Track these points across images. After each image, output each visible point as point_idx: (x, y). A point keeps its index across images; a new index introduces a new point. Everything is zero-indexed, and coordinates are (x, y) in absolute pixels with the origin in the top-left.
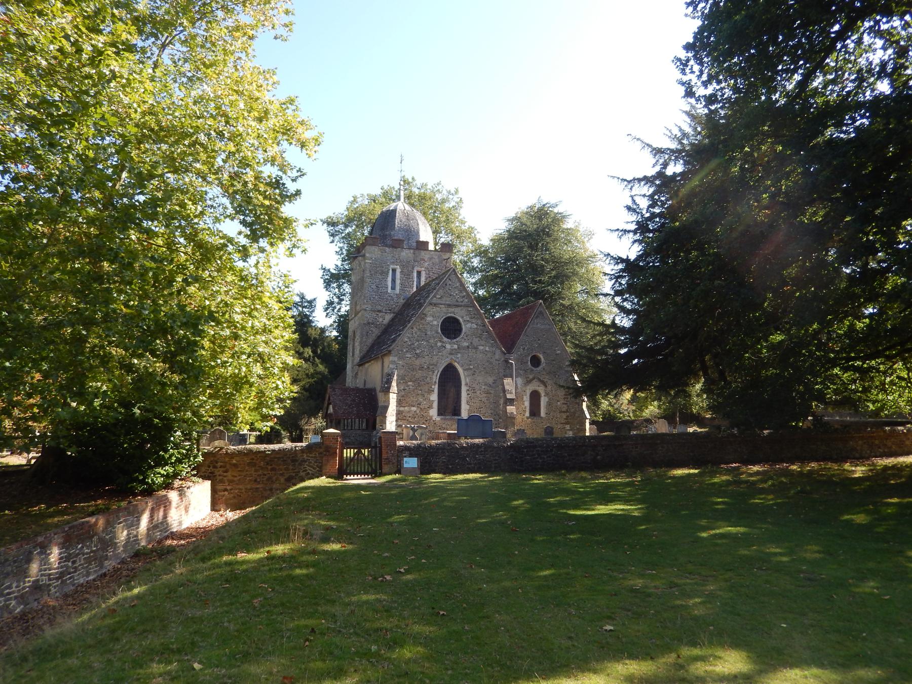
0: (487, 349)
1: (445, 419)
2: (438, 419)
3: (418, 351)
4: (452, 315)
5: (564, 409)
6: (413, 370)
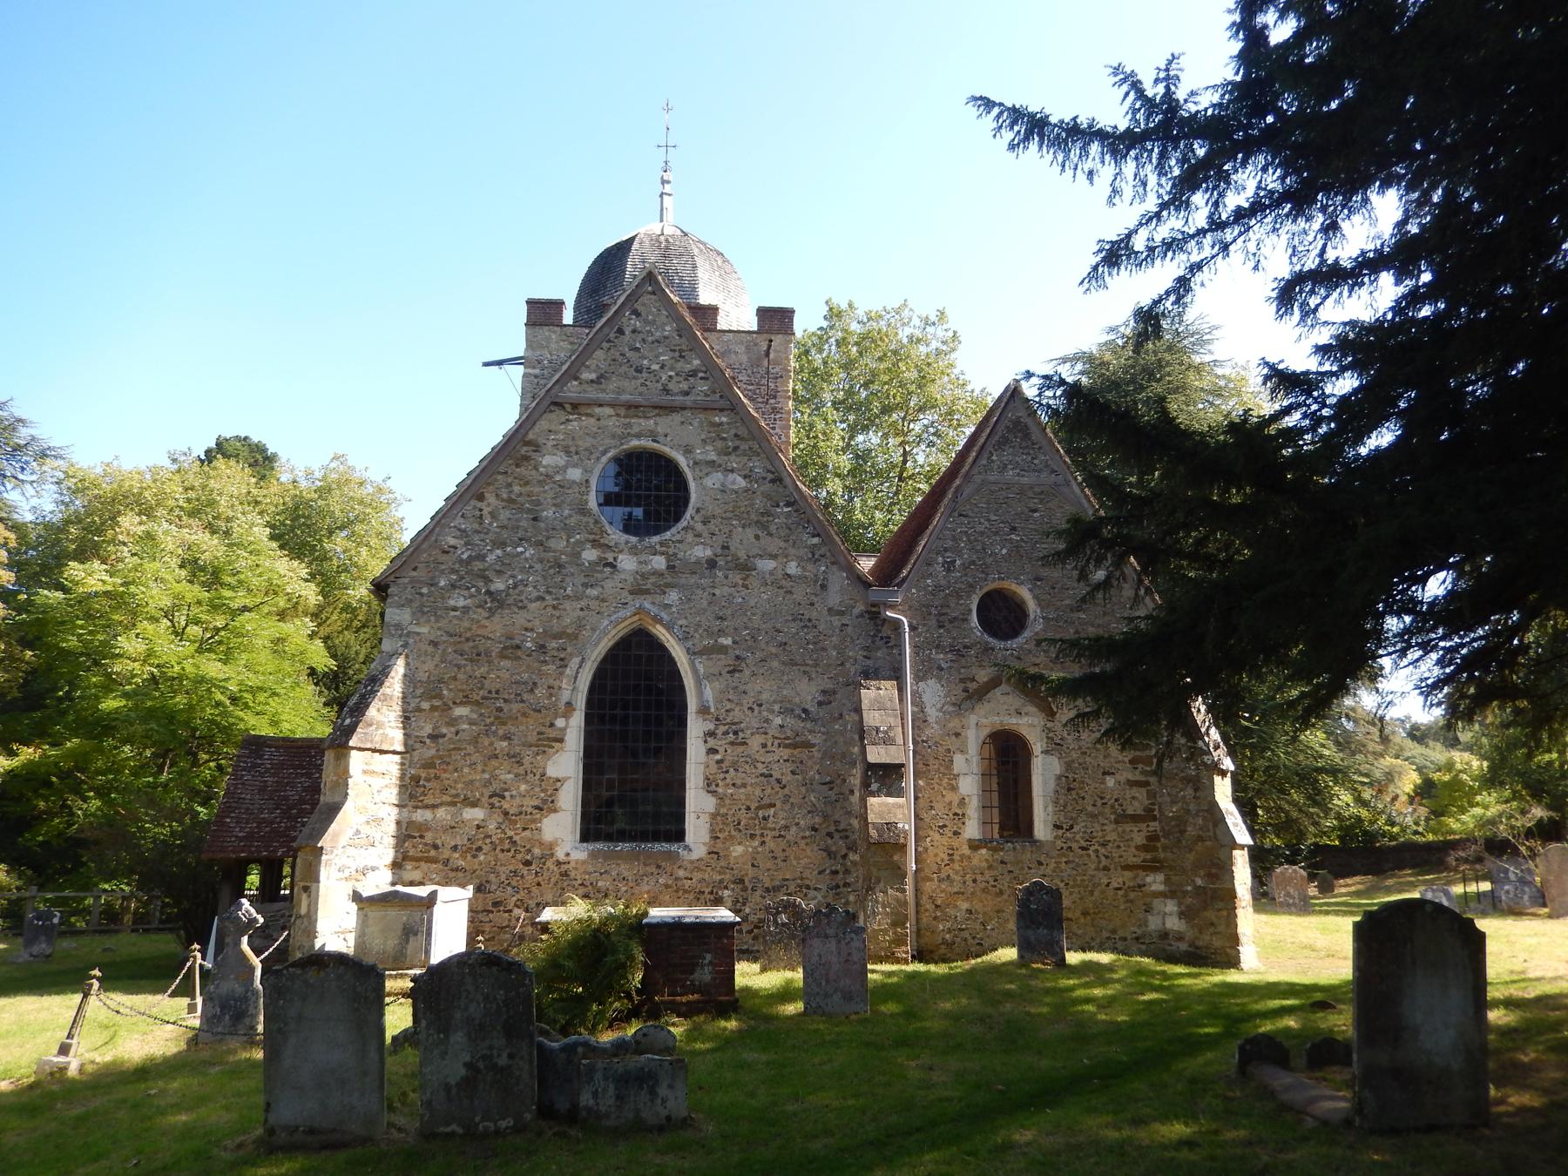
0: (793, 568)
1: (608, 856)
2: (580, 854)
3: (499, 585)
4: (646, 443)
5: (1135, 808)
6: (477, 657)
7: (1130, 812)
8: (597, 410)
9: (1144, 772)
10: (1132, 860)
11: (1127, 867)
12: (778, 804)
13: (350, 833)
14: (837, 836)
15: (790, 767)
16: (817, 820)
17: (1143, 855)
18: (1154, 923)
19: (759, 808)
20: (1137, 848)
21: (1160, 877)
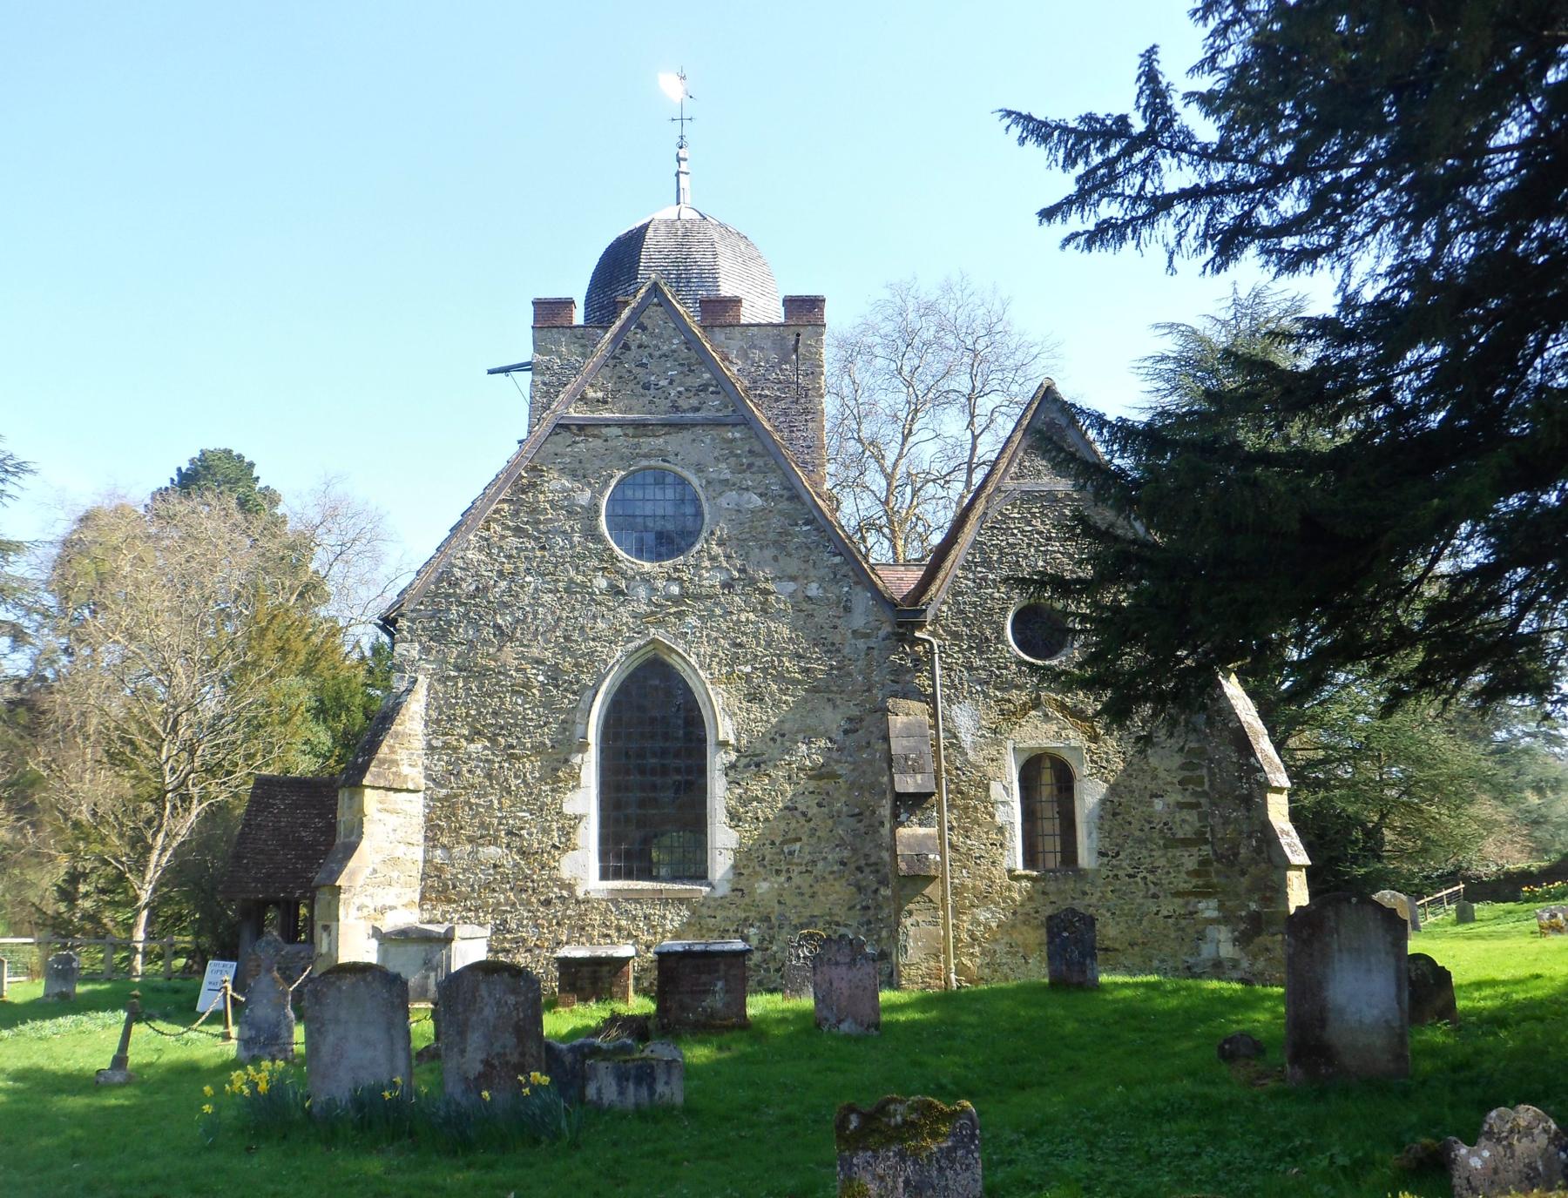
0: (813, 590)
7: (1180, 835)
8: (605, 431)
9: (1194, 793)
10: (1183, 886)
11: (1177, 894)
12: (804, 838)
13: (367, 872)
14: (867, 870)
16: (846, 854)
17: (1194, 881)
18: (1207, 951)
19: (782, 843)
20: (1188, 873)
21: (1213, 903)
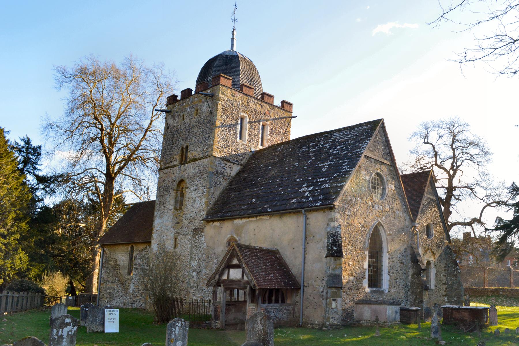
5: (444, 282)
11: (443, 296)
15: (400, 268)
